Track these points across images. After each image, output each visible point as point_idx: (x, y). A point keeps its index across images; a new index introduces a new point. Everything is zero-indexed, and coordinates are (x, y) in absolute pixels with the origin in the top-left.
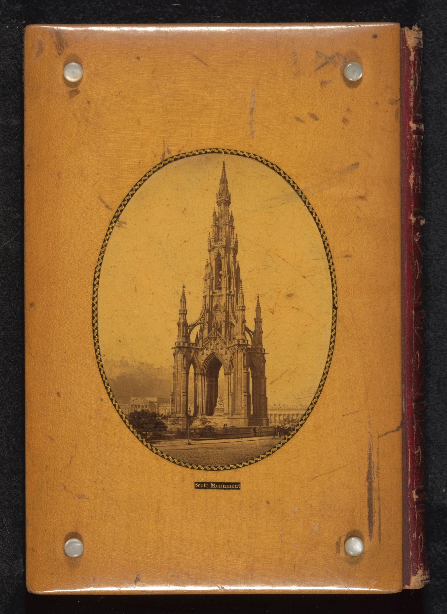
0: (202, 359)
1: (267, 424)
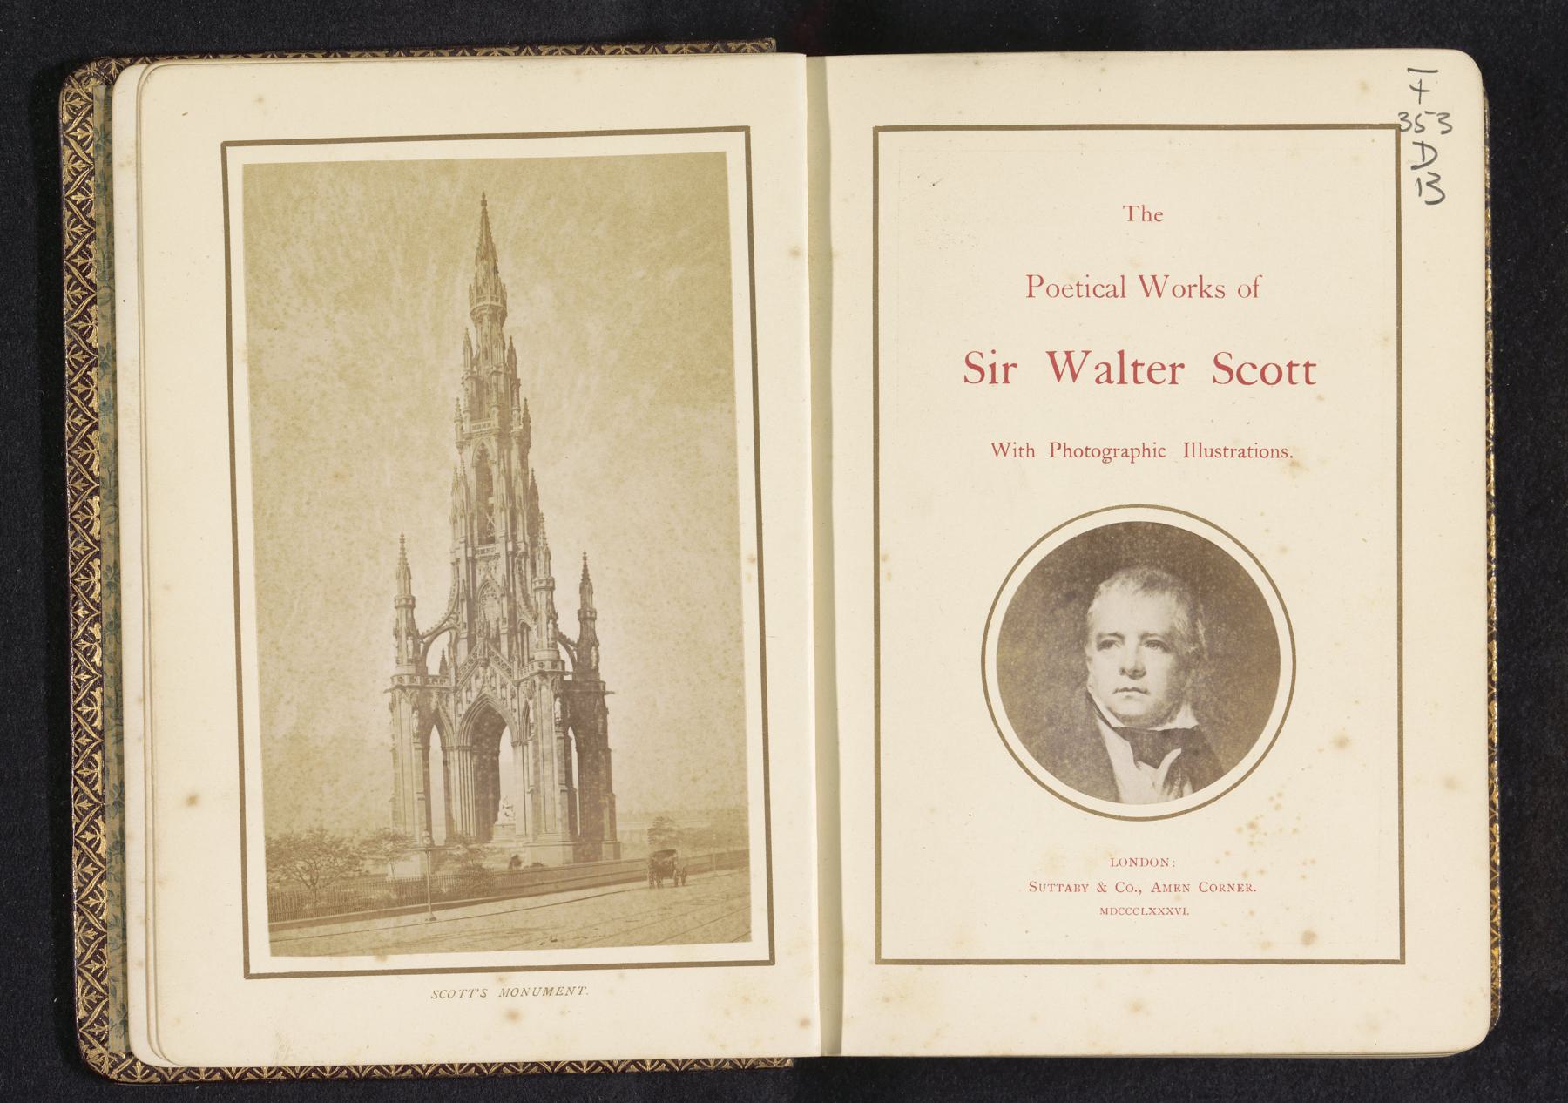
0: (457, 710)
1: (617, 855)
